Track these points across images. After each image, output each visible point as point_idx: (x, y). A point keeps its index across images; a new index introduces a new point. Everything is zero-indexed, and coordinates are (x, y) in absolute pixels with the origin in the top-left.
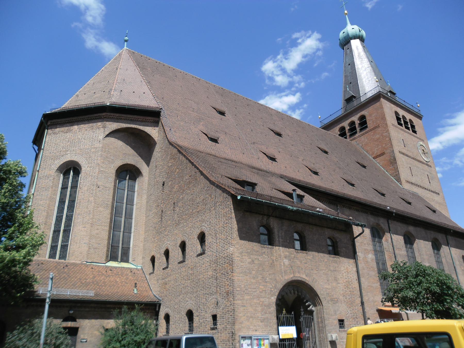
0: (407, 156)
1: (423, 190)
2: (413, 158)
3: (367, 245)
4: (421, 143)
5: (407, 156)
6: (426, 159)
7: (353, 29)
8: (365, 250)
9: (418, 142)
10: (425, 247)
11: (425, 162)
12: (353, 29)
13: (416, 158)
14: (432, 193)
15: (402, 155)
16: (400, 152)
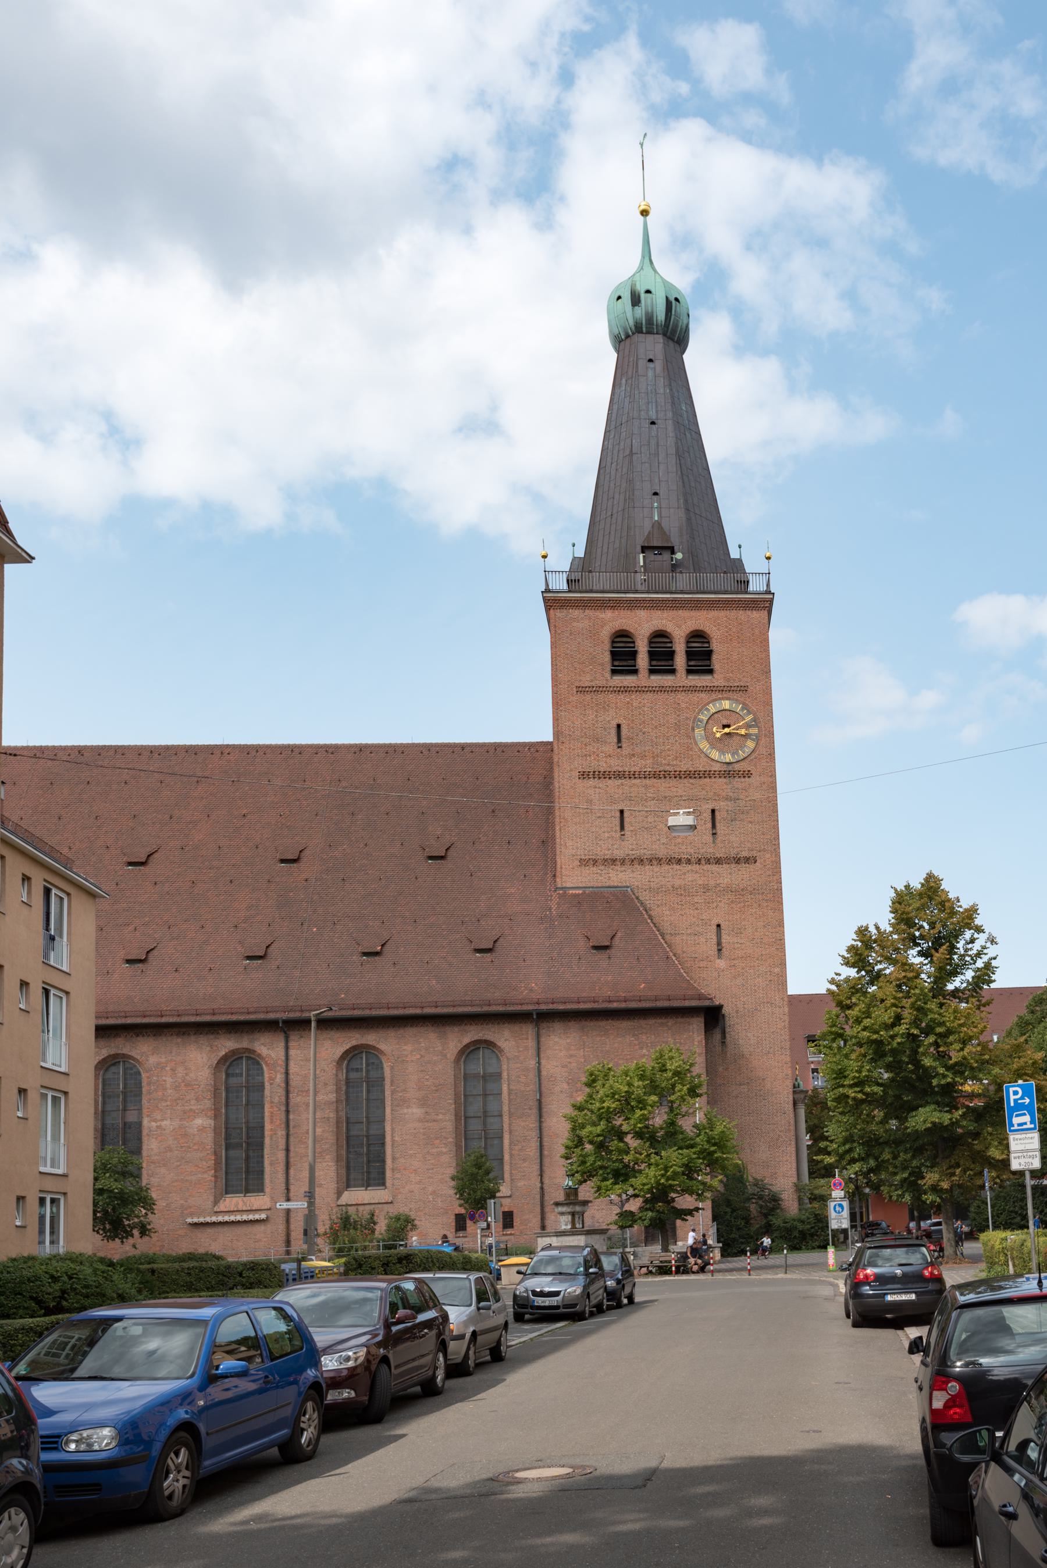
0: (620, 775)
1: (666, 867)
2: (656, 775)
3: (193, 1102)
4: (726, 704)
5: (620, 775)
6: (728, 758)
7: (619, 298)
8: (185, 1112)
9: (708, 704)
10: (422, 1071)
11: (717, 767)
12: (619, 298)
13: (668, 768)
14: (714, 868)
15: (592, 782)
16: (584, 775)
